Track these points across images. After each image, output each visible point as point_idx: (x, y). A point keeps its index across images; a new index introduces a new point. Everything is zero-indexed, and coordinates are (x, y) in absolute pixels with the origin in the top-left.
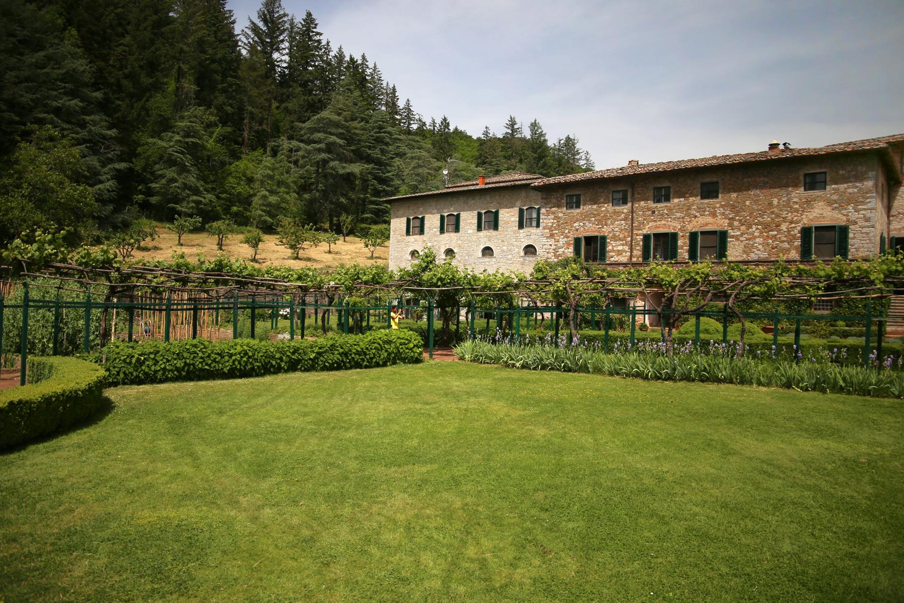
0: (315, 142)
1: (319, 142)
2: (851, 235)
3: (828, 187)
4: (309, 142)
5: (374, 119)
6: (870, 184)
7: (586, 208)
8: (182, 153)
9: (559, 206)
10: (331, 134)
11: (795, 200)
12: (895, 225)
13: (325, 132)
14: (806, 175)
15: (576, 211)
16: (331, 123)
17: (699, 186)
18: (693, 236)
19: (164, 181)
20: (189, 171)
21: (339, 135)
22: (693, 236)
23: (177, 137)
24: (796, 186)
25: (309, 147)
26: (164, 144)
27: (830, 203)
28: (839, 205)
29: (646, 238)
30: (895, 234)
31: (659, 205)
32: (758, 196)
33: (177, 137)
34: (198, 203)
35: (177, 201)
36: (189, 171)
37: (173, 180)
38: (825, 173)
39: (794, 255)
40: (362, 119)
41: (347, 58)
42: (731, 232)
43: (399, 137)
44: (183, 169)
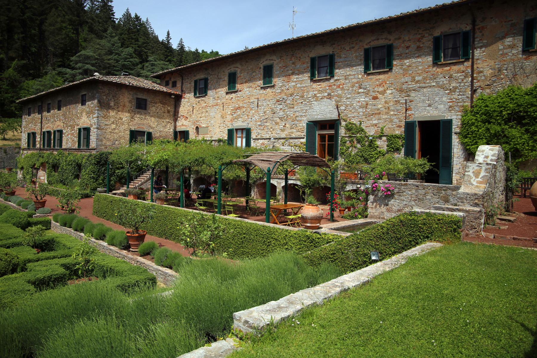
0: (76, 69)
1: (80, 69)
3: (87, 103)
4: (73, 69)
5: (124, 53)
6: (96, 101)
7: (32, 115)
9: (26, 115)
10: (87, 64)
12: (179, 124)
13: (84, 63)
14: (83, 96)
15: (30, 117)
16: (88, 57)
17: (57, 102)
18: (55, 132)
21: (93, 65)
22: (55, 132)
24: (79, 103)
25: (73, 72)
27: (87, 113)
28: (89, 114)
29: (44, 132)
30: (179, 129)
31: (49, 114)
32: (70, 109)
38: (85, 95)
40: (117, 54)
41: (133, 16)
42: (64, 131)
43: (153, 62)
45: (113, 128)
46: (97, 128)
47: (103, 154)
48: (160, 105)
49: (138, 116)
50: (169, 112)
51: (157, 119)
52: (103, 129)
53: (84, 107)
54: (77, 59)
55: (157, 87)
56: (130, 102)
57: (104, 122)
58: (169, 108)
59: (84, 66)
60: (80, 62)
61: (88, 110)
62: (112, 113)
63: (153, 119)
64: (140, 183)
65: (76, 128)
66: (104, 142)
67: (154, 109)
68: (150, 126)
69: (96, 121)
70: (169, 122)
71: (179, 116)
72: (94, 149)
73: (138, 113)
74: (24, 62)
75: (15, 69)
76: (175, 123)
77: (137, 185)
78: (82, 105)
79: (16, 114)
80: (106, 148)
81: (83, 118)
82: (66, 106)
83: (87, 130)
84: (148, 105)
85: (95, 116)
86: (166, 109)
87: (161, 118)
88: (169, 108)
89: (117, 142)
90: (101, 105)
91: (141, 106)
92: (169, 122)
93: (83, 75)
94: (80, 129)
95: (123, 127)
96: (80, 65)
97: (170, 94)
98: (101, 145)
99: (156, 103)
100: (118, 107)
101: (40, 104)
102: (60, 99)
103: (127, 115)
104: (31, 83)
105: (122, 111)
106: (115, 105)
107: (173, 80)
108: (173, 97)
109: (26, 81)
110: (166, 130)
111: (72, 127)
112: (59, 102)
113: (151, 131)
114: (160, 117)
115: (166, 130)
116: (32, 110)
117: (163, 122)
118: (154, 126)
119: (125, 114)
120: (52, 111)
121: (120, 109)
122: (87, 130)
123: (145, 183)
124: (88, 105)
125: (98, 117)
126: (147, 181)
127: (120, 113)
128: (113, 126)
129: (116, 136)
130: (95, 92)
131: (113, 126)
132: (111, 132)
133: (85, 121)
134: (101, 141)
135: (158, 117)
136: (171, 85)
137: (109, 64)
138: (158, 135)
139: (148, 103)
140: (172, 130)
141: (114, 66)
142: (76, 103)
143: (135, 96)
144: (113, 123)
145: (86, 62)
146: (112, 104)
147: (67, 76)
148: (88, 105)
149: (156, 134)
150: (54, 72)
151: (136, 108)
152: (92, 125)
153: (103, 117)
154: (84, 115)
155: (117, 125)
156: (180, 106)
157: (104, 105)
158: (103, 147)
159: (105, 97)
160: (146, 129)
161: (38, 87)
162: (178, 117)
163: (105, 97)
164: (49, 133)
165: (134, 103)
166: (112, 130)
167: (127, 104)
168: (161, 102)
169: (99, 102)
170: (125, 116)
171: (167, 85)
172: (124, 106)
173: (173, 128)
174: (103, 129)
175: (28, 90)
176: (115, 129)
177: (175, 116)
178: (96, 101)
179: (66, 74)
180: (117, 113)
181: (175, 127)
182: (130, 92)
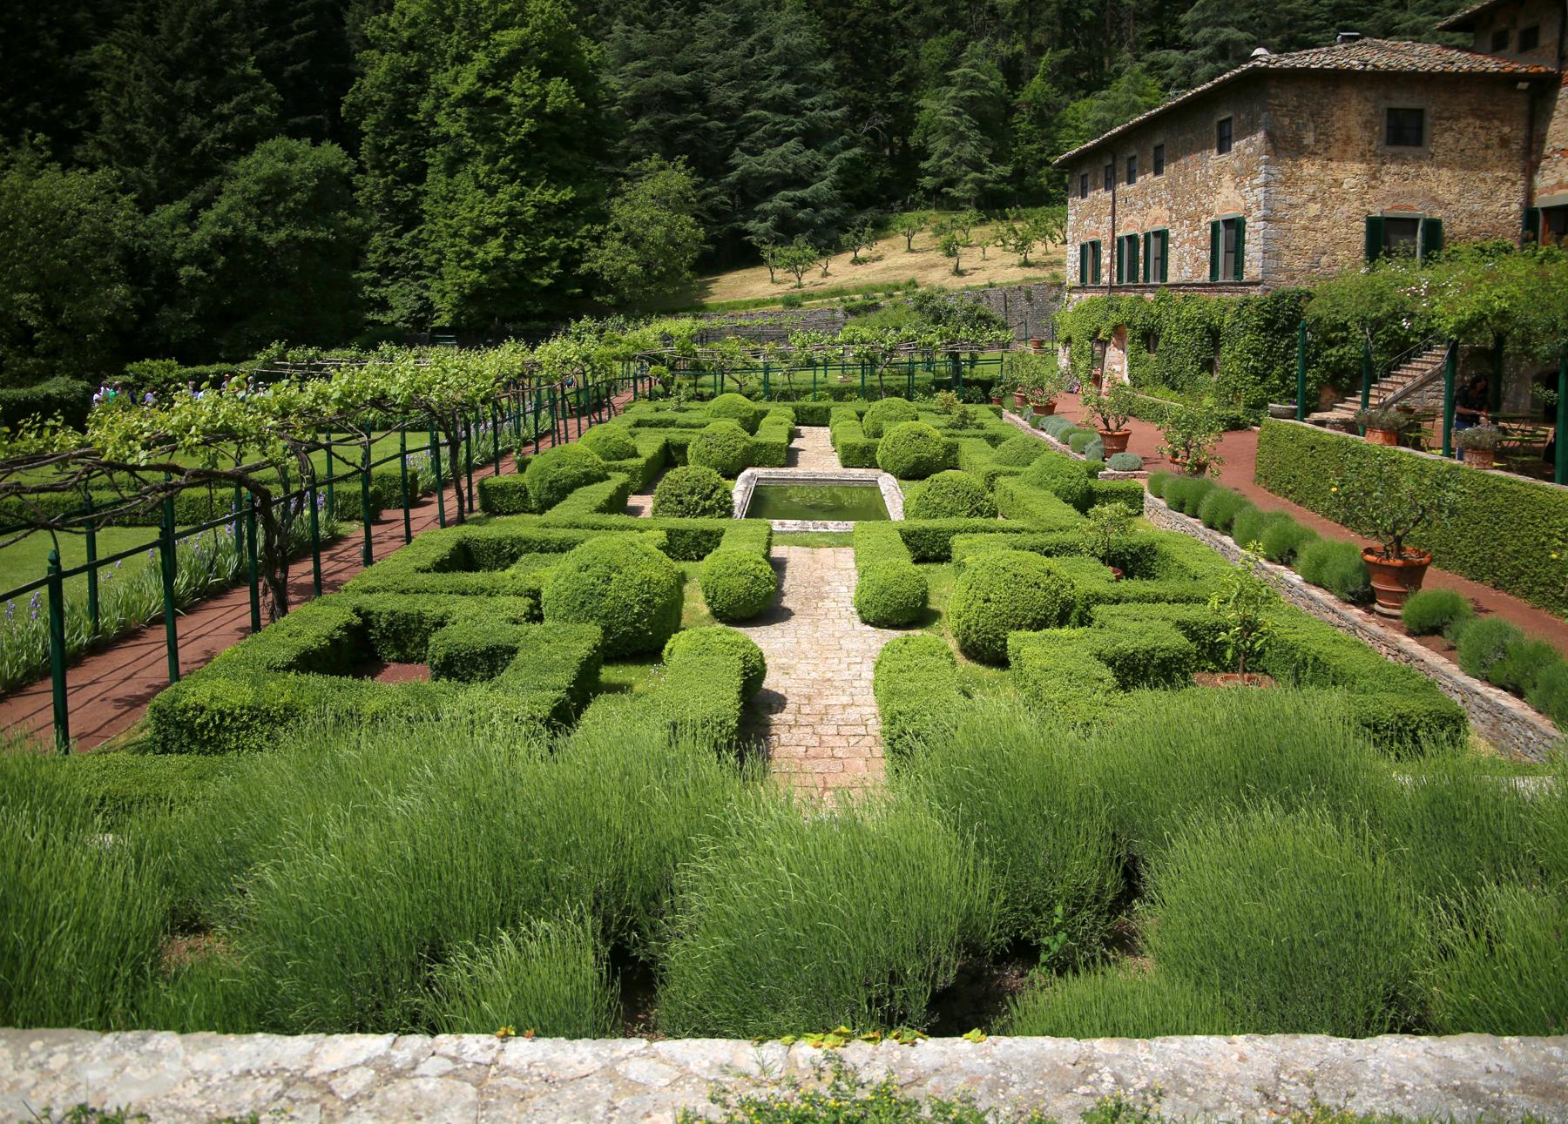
0: (1195, 46)
1: (1205, 44)
2: (1247, 236)
3: (1235, 145)
4: (1187, 47)
6: (1261, 135)
8: (956, 114)
10: (1225, 25)
11: (1211, 172)
19: (935, 157)
20: (967, 138)
21: (1242, 26)
23: (952, 93)
24: (1211, 148)
25: (1188, 57)
26: (935, 105)
27: (1235, 175)
28: (1240, 176)
30: (1542, 201)
31: (1132, 187)
32: (1186, 167)
33: (953, 92)
34: (980, 184)
35: (951, 183)
36: (967, 138)
37: (946, 154)
38: (1229, 120)
39: (1206, 275)
44: (962, 137)
45: (1311, 214)
46: (1266, 219)
47: (1283, 296)
48: (1472, 124)
49: (1394, 168)
50: (1504, 142)
51: (1460, 173)
52: (1282, 220)
53: (1225, 157)
54: (1198, 16)
55: (1463, 62)
56: (1367, 125)
57: (1285, 196)
58: (1506, 130)
59: (1217, 34)
60: (1205, 22)
61: (1237, 164)
62: (1309, 168)
63: (1445, 174)
64: (1399, 390)
65: (1205, 222)
66: (1286, 259)
67: (1448, 138)
68: (1434, 199)
69: (1261, 197)
70: (1505, 179)
71: (1547, 152)
72: (1258, 284)
73: (1394, 158)
74: (1066, 52)
75: (1044, 77)
76: (1530, 180)
77: (1390, 396)
78: (1220, 152)
79: (1049, 195)
80: (1293, 278)
81: (1224, 191)
82: (1175, 159)
83: (1236, 226)
84: (1427, 127)
85: (1260, 180)
86: (1494, 133)
87: (1478, 168)
88: (1506, 130)
89: (1324, 259)
90: (1275, 147)
91: (1403, 134)
92: (1505, 179)
93: (1215, 62)
94: (1215, 226)
95: (1345, 208)
96: (1205, 32)
97: (1511, 79)
98: (1278, 270)
99: (1456, 118)
100: (1326, 149)
101: (1109, 162)
102: (1158, 141)
103: (1358, 167)
104: (1082, 105)
105: (1342, 160)
106: (1317, 141)
107: (1522, 25)
108: (1522, 86)
109: (1073, 105)
110: (1495, 207)
111: (1194, 219)
112: (1159, 149)
113: (1438, 214)
114: (1470, 163)
115: (1495, 207)
116: (1090, 180)
117: (1483, 180)
118: (1448, 197)
119: (1349, 166)
120: (1139, 179)
121: (1334, 152)
122: (1236, 226)
123: (1416, 390)
124: (1238, 150)
125: (1266, 185)
126: (1423, 385)
127: (1334, 165)
128: (1314, 209)
129: (1322, 240)
130: (1257, 108)
131: (1314, 209)
132: (1305, 228)
133: (1228, 200)
134: (1278, 256)
135: (1466, 166)
136: (1513, 45)
137: (1289, 12)
138: (1463, 228)
139: (1428, 120)
140: (1515, 207)
141: (1306, 17)
142: (1203, 148)
143: (1384, 105)
144: (1313, 199)
145: (1223, 19)
146: (1309, 139)
147: (1171, 71)
148: (1238, 150)
149: (1455, 225)
150: (1138, 67)
151: (1388, 143)
152: (1248, 211)
153: (1282, 183)
154: (1226, 182)
155: (1324, 204)
156: (1549, 117)
157: (1284, 147)
158: (1282, 277)
159: (1286, 121)
160: (1420, 210)
161: (1101, 115)
162: (1541, 157)
163: (1286, 121)
164: (1132, 239)
165: (1380, 127)
166: (1311, 220)
167: (1357, 133)
168: (1474, 113)
169: (1270, 137)
170: (1351, 174)
171: (1498, 46)
172: (1348, 141)
173: (1520, 198)
174: (1282, 220)
175: (1076, 128)
176: (1317, 218)
177: (1531, 156)
178: (1261, 135)
179: (1169, 66)
180: (1324, 167)
181: (1529, 194)
182: (1367, 94)
